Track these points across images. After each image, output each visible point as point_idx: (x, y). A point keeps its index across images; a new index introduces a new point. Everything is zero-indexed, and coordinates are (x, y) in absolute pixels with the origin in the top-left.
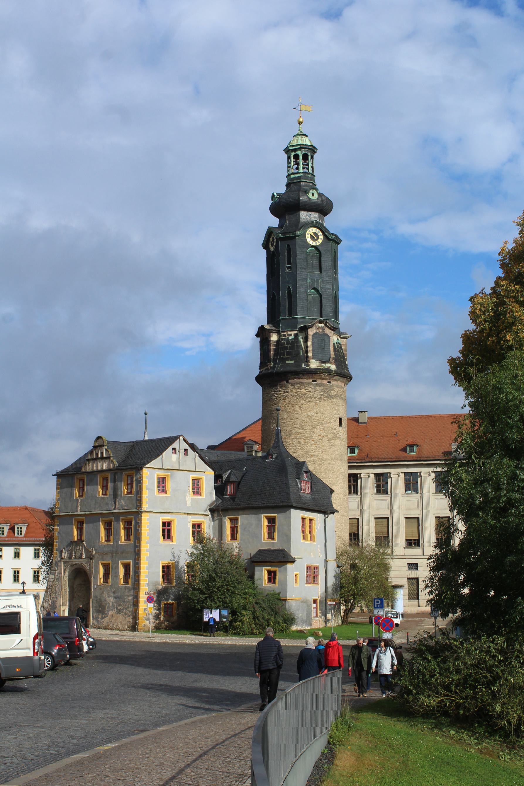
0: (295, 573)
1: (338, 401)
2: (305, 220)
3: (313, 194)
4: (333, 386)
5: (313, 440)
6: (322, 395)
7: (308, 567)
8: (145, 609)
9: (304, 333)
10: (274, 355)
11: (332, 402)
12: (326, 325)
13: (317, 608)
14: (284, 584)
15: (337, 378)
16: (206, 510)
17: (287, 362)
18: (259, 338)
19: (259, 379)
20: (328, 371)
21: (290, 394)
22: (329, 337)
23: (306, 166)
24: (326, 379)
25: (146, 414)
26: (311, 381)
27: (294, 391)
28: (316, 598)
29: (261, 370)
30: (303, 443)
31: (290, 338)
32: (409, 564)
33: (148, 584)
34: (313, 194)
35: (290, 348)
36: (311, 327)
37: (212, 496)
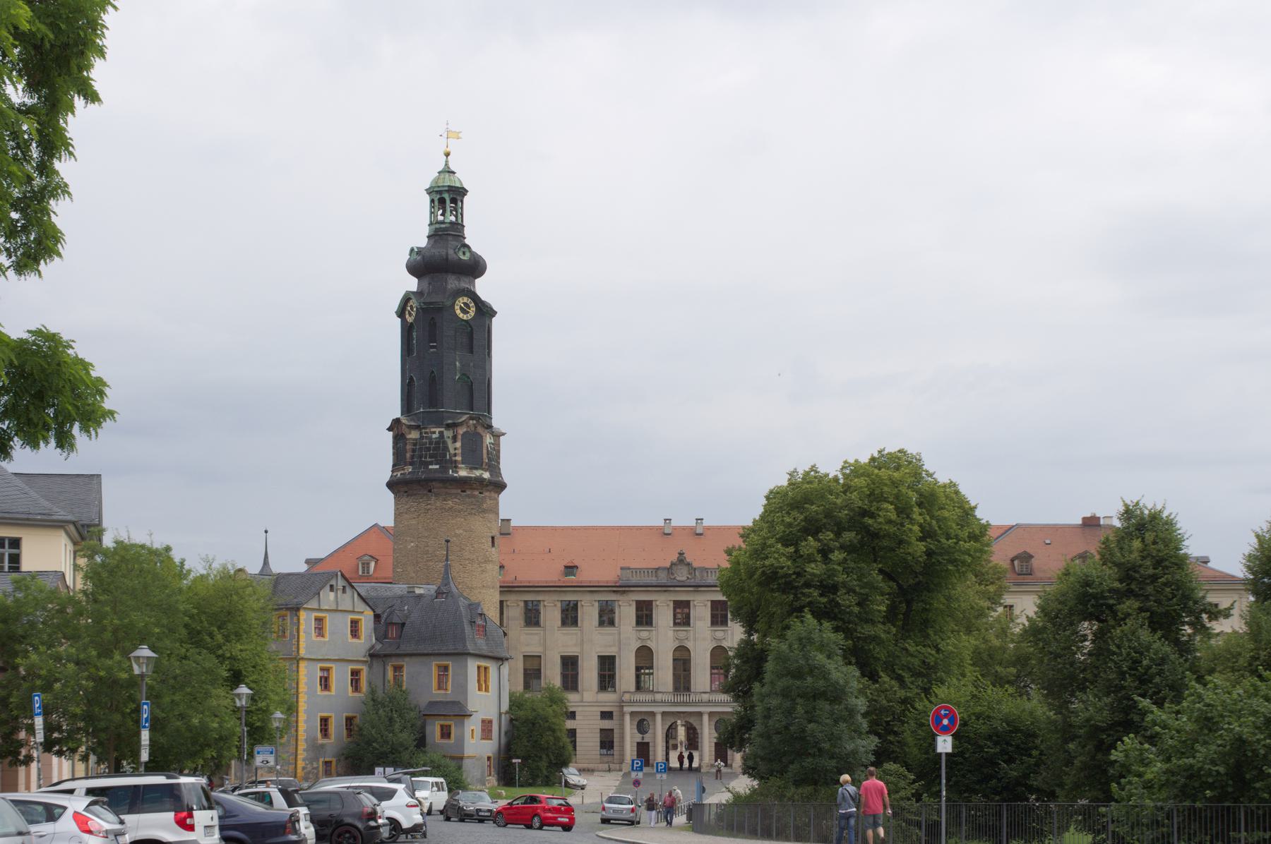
0: (472, 728)
1: (490, 516)
2: (453, 286)
4: (485, 497)
7: (483, 721)
8: (304, 768)
9: (452, 431)
10: (412, 457)
11: (484, 518)
12: (478, 421)
14: (461, 740)
17: (430, 467)
18: (391, 433)
19: (391, 485)
20: (480, 481)
21: (434, 507)
22: (482, 437)
24: (477, 489)
25: (266, 532)
26: (459, 491)
27: (438, 504)
28: (490, 755)
29: (395, 474)
31: (434, 436)
33: (306, 740)
35: (435, 449)
36: (461, 424)
37: (371, 640)
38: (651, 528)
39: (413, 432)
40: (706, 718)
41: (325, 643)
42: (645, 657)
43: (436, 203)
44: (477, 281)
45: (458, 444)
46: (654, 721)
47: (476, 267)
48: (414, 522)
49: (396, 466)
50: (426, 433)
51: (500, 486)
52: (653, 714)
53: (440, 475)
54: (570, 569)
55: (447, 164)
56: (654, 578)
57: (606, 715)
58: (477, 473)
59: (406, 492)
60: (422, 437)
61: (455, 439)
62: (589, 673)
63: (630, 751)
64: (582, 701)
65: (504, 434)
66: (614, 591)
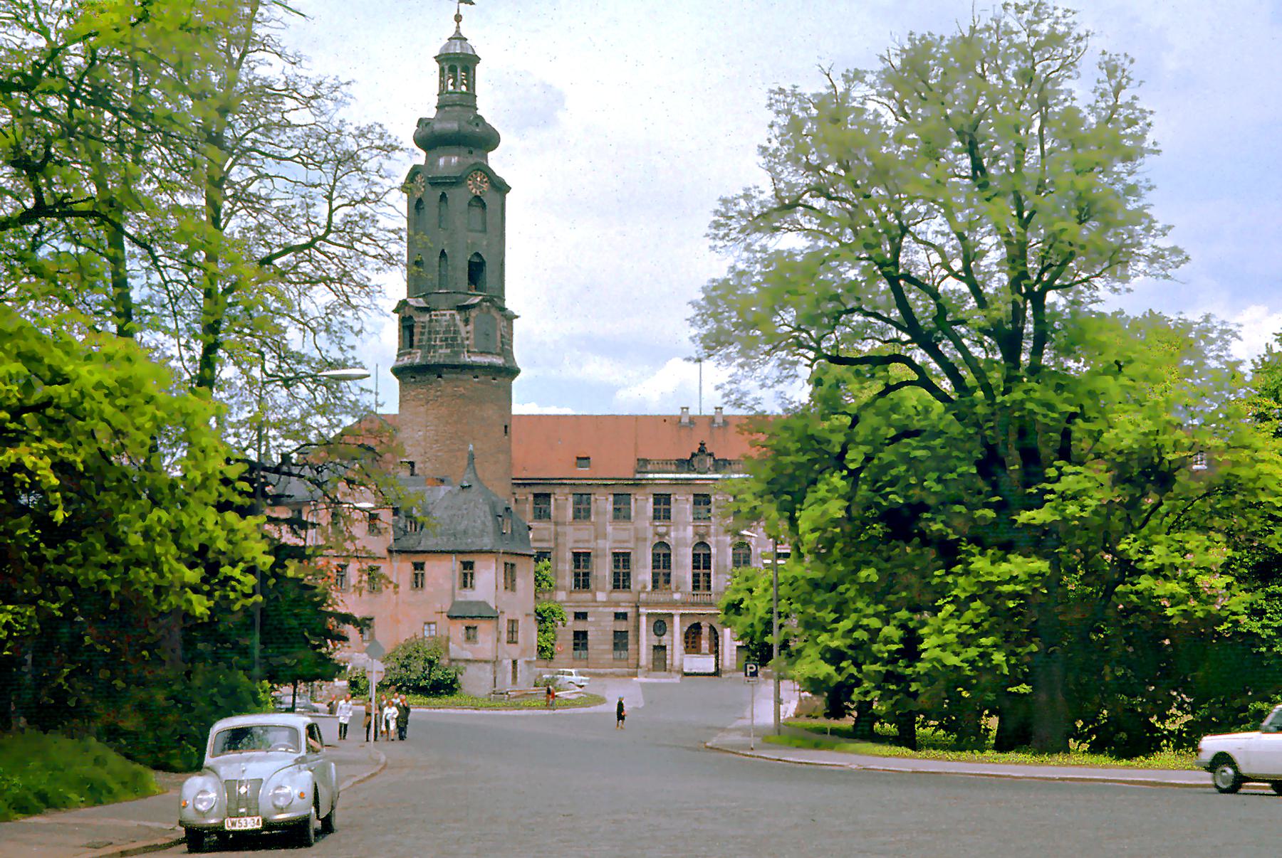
38: (665, 419)
42: (662, 559)
43: (446, 71)
44: (490, 155)
46: (672, 622)
47: (489, 140)
50: (436, 315)
51: (513, 372)
52: (671, 615)
54: (583, 460)
55: (458, 31)
57: (620, 616)
62: (603, 570)
63: (645, 656)
64: (596, 601)
65: (517, 317)
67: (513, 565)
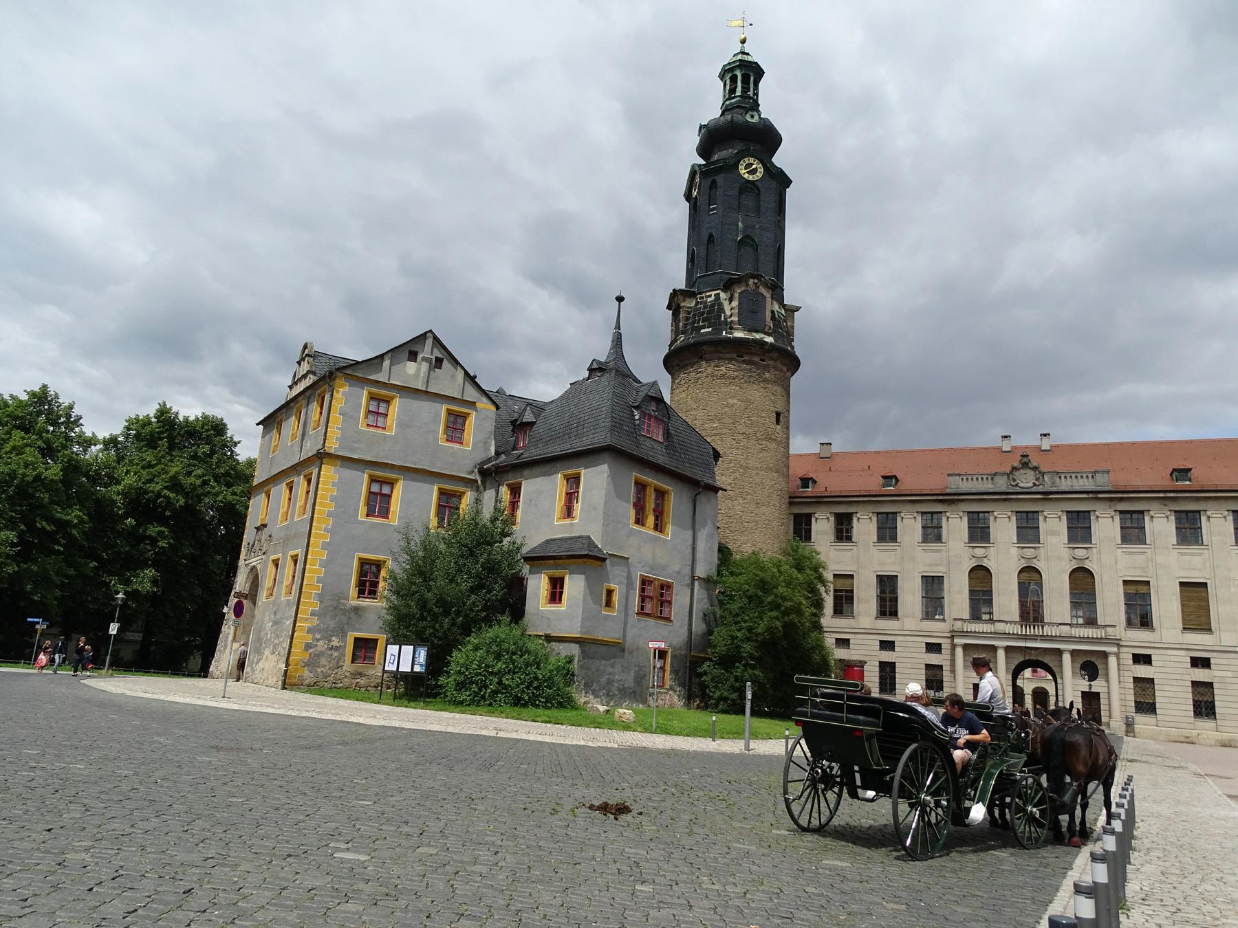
3: (752, 117)
5: (734, 439)
6: (750, 376)
8: (308, 646)
9: (729, 293)
10: (685, 326)
11: (766, 388)
13: (663, 668)
15: (775, 355)
16: (473, 472)
17: (702, 331)
20: (761, 343)
22: (764, 297)
23: (745, 89)
24: (759, 355)
26: (735, 355)
27: (710, 371)
30: (719, 443)
31: (709, 300)
32: (881, 642)
34: (752, 117)
37: (488, 449)
39: (687, 300)
40: (1067, 658)
41: (385, 437)
45: (735, 303)
48: (683, 395)
49: (670, 346)
53: (712, 337)
54: (889, 478)
56: (990, 486)
58: (758, 336)
59: (679, 365)
60: (697, 303)
61: (731, 300)
65: (798, 309)
66: (940, 501)
67: (661, 494)
